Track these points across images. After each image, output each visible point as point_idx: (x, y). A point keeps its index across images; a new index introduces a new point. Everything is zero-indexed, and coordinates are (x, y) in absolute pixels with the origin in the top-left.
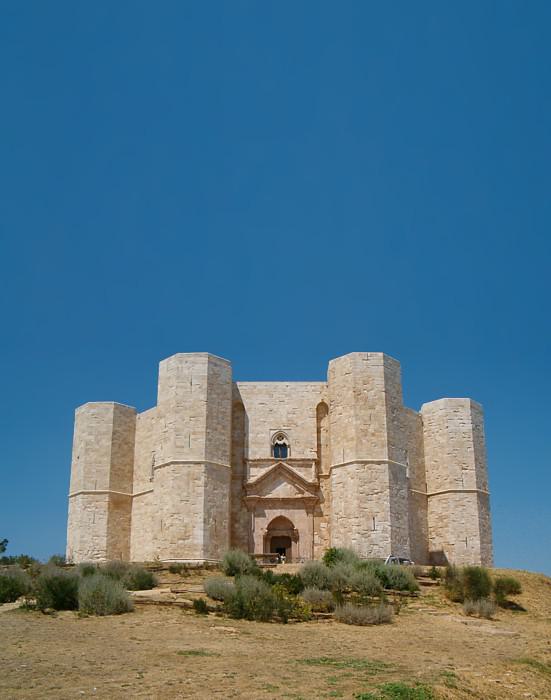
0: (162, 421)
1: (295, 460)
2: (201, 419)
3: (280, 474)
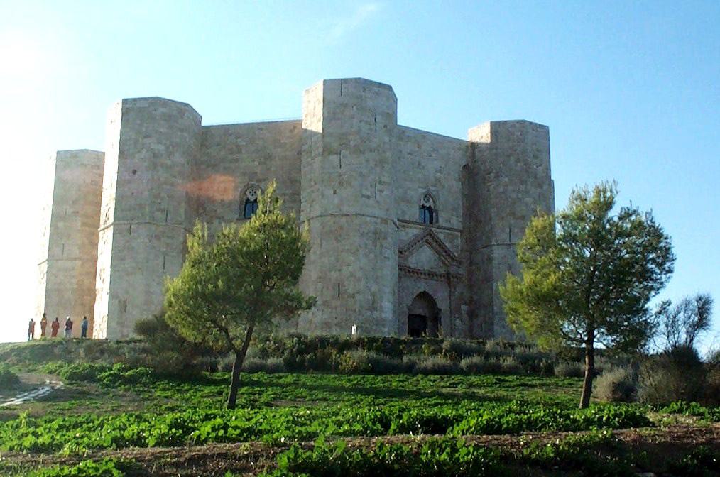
0: (335, 158)
1: (445, 228)
2: (386, 165)
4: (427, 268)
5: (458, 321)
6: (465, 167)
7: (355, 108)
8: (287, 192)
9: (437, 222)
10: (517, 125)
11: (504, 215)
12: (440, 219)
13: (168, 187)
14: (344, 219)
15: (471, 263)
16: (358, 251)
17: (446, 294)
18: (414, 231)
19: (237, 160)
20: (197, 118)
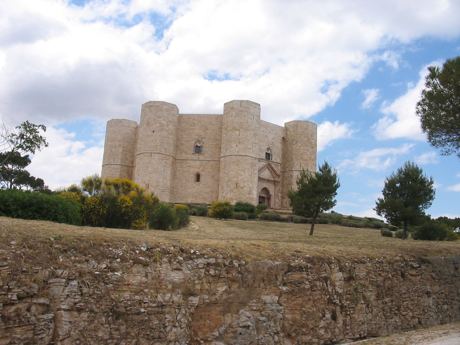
0: (237, 132)
2: (257, 137)
3: (267, 167)
6: (283, 138)
7: (246, 112)
8: (213, 144)
9: (272, 159)
10: (306, 123)
11: (298, 158)
12: (273, 159)
13: (167, 139)
14: (240, 158)
15: (283, 177)
16: (245, 170)
18: (263, 164)
19: (193, 129)
20: (178, 110)
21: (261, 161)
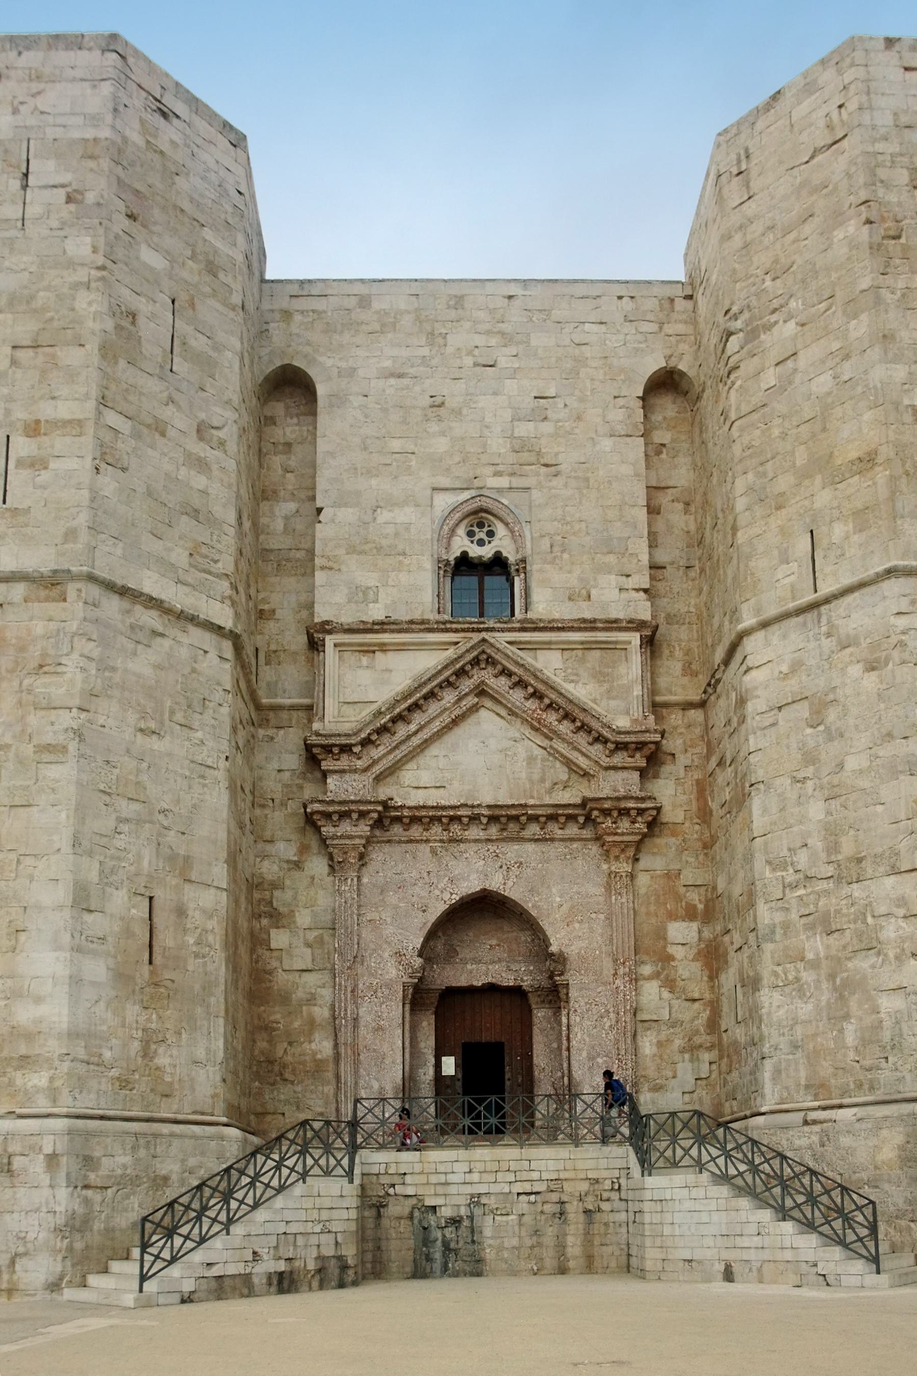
4: (487, 798)
5: (652, 993)
17: (595, 890)
21: (383, 648)
